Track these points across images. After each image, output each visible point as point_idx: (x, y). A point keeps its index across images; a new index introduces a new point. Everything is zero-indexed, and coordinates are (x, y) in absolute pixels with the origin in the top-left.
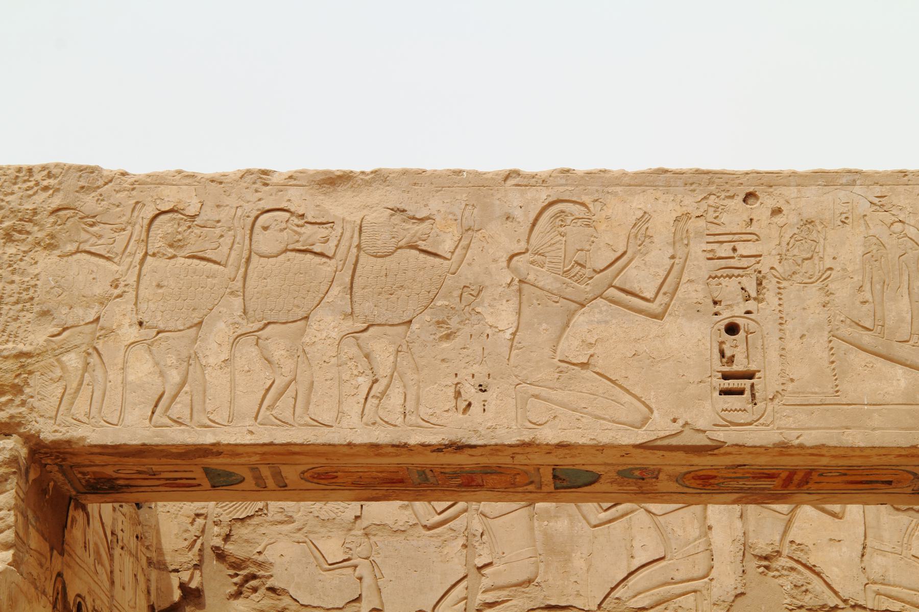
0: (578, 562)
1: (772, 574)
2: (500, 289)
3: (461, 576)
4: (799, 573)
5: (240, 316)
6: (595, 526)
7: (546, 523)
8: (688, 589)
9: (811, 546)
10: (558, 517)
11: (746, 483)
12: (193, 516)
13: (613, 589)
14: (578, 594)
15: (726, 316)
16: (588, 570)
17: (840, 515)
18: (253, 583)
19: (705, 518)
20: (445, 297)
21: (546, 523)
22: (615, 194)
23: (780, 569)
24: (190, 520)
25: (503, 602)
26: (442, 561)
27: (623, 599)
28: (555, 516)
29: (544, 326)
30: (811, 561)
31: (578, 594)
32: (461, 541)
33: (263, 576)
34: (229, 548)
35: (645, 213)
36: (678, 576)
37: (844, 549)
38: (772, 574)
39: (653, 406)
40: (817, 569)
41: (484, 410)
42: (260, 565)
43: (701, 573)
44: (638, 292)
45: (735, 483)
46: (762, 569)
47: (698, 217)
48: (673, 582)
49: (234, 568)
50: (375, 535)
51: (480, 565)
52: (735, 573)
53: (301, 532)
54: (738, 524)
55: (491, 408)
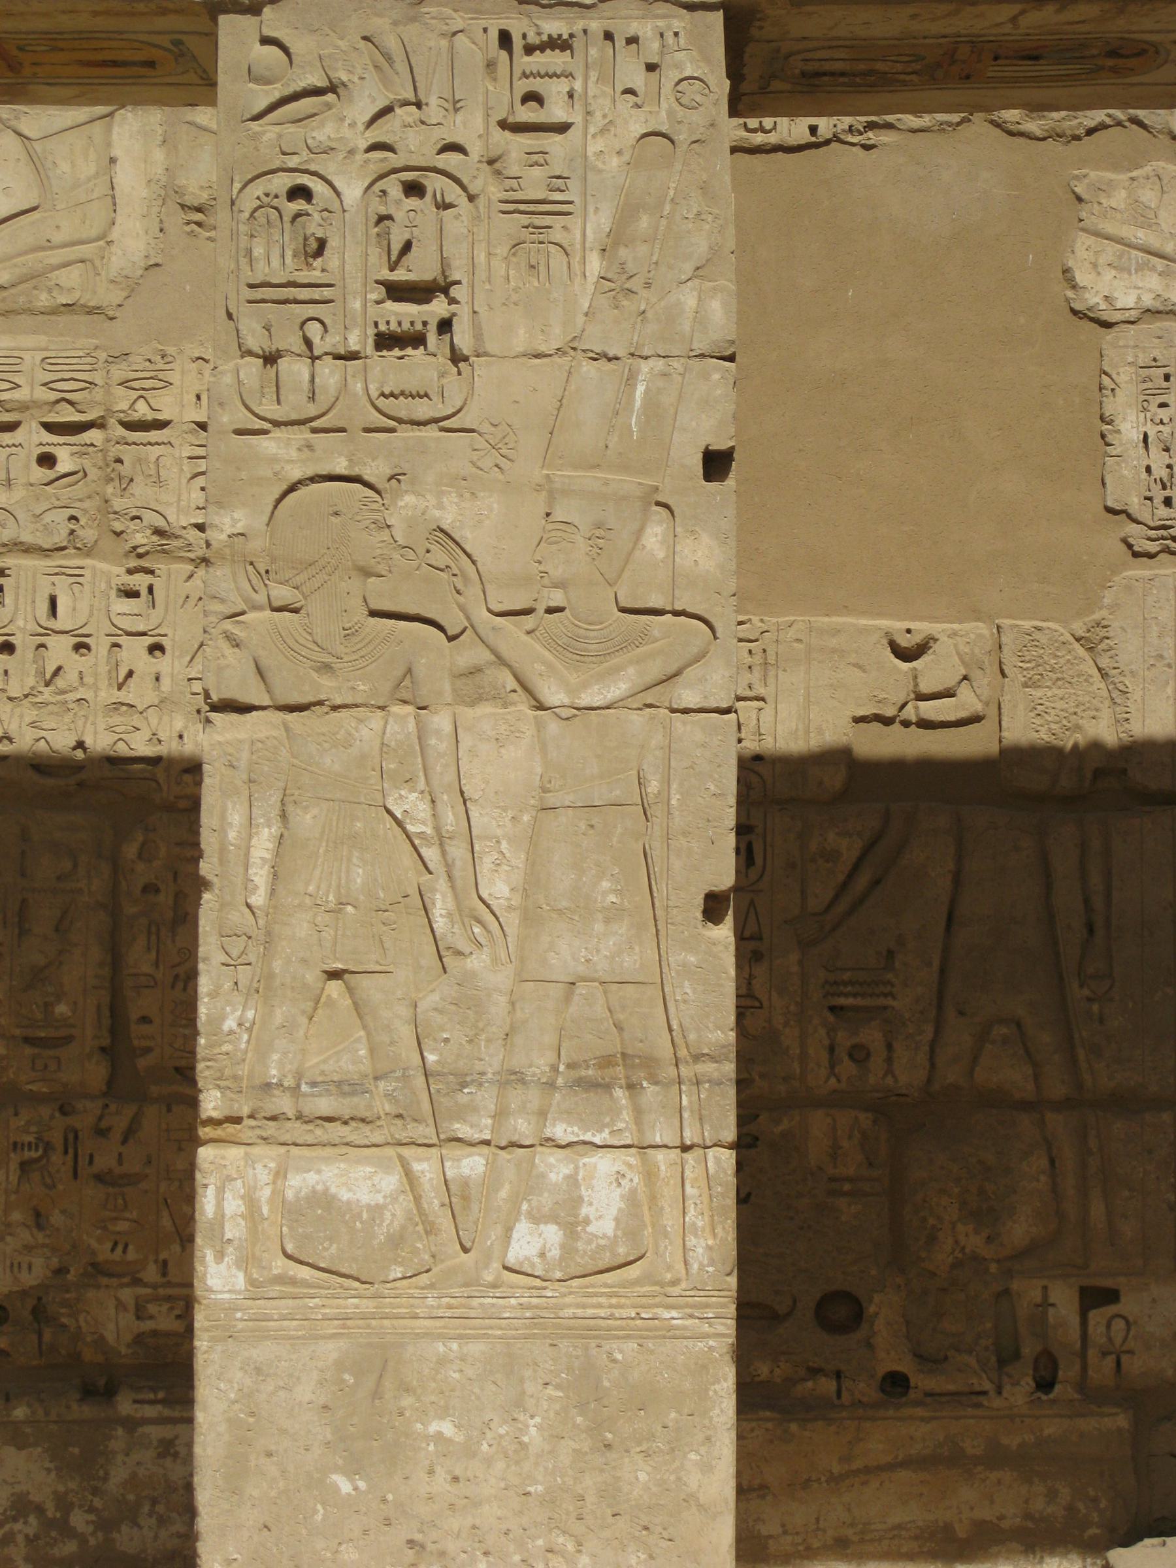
8: (72, 257)
19: (109, 145)
36: (57, 238)
43: (94, 233)
46: (194, 227)
48: (49, 246)
52: (147, 232)
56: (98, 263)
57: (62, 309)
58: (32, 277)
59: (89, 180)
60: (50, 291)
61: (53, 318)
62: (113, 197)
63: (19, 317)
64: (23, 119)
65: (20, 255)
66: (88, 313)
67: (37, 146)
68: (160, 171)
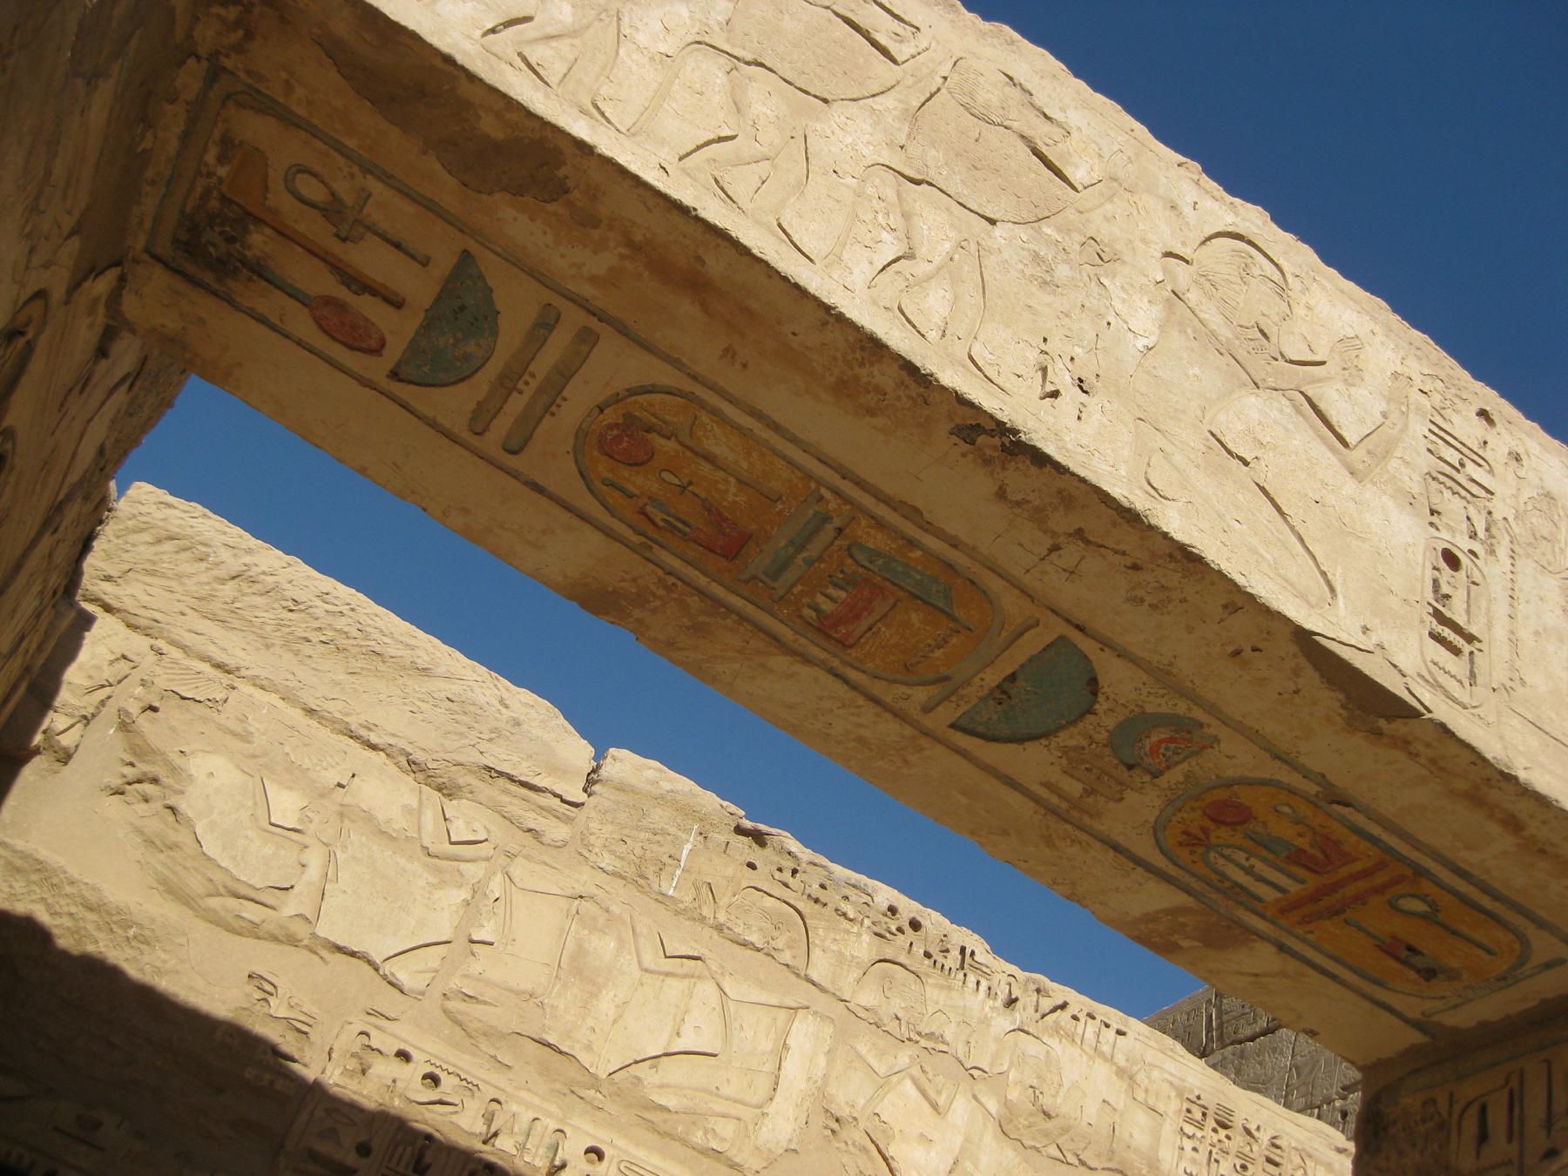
0: (605, 1006)
1: (837, 1145)
2: (1144, 280)
3: (444, 939)
4: (871, 1159)
5: (719, 23)
6: (646, 970)
7: (586, 932)
8: (733, 1112)
9: (897, 1131)
10: (604, 933)
11: (1259, 866)
12: (119, 656)
13: (636, 1062)
14: (589, 1048)
15: (1445, 538)
16: (615, 1021)
17: (941, 1110)
18: (148, 788)
20: (1059, 229)
21: (586, 932)
22: (1324, 288)
23: (849, 1143)
24: (113, 658)
25: (485, 1003)
26: (427, 906)
27: (645, 1083)
28: (601, 930)
29: (1196, 370)
30: (891, 1151)
31: (589, 1048)
32: (465, 894)
33: (169, 787)
34: (144, 723)
35: (1357, 337)
36: (726, 1090)
37: (933, 1154)
38: (837, 1145)
39: (1338, 589)
40: (894, 1165)
41: (1079, 418)
42: (175, 770)
43: (755, 1100)
44: (1334, 423)
45: (1240, 857)
47: (1422, 391)
48: (716, 1093)
49: (135, 754)
50: (353, 821)
51: (475, 938)
53: (255, 760)
54: (822, 1061)
55: (1094, 417)
56: (751, 1127)
57: (711, 1152)
58: (695, 1116)
59: (764, 1054)
60: (706, 1132)
61: (700, 1156)
62: (777, 1077)
63: (673, 1142)
64: (727, 978)
65: (690, 1088)
66: (731, 1167)
67: (732, 1007)
68: (819, 1074)
